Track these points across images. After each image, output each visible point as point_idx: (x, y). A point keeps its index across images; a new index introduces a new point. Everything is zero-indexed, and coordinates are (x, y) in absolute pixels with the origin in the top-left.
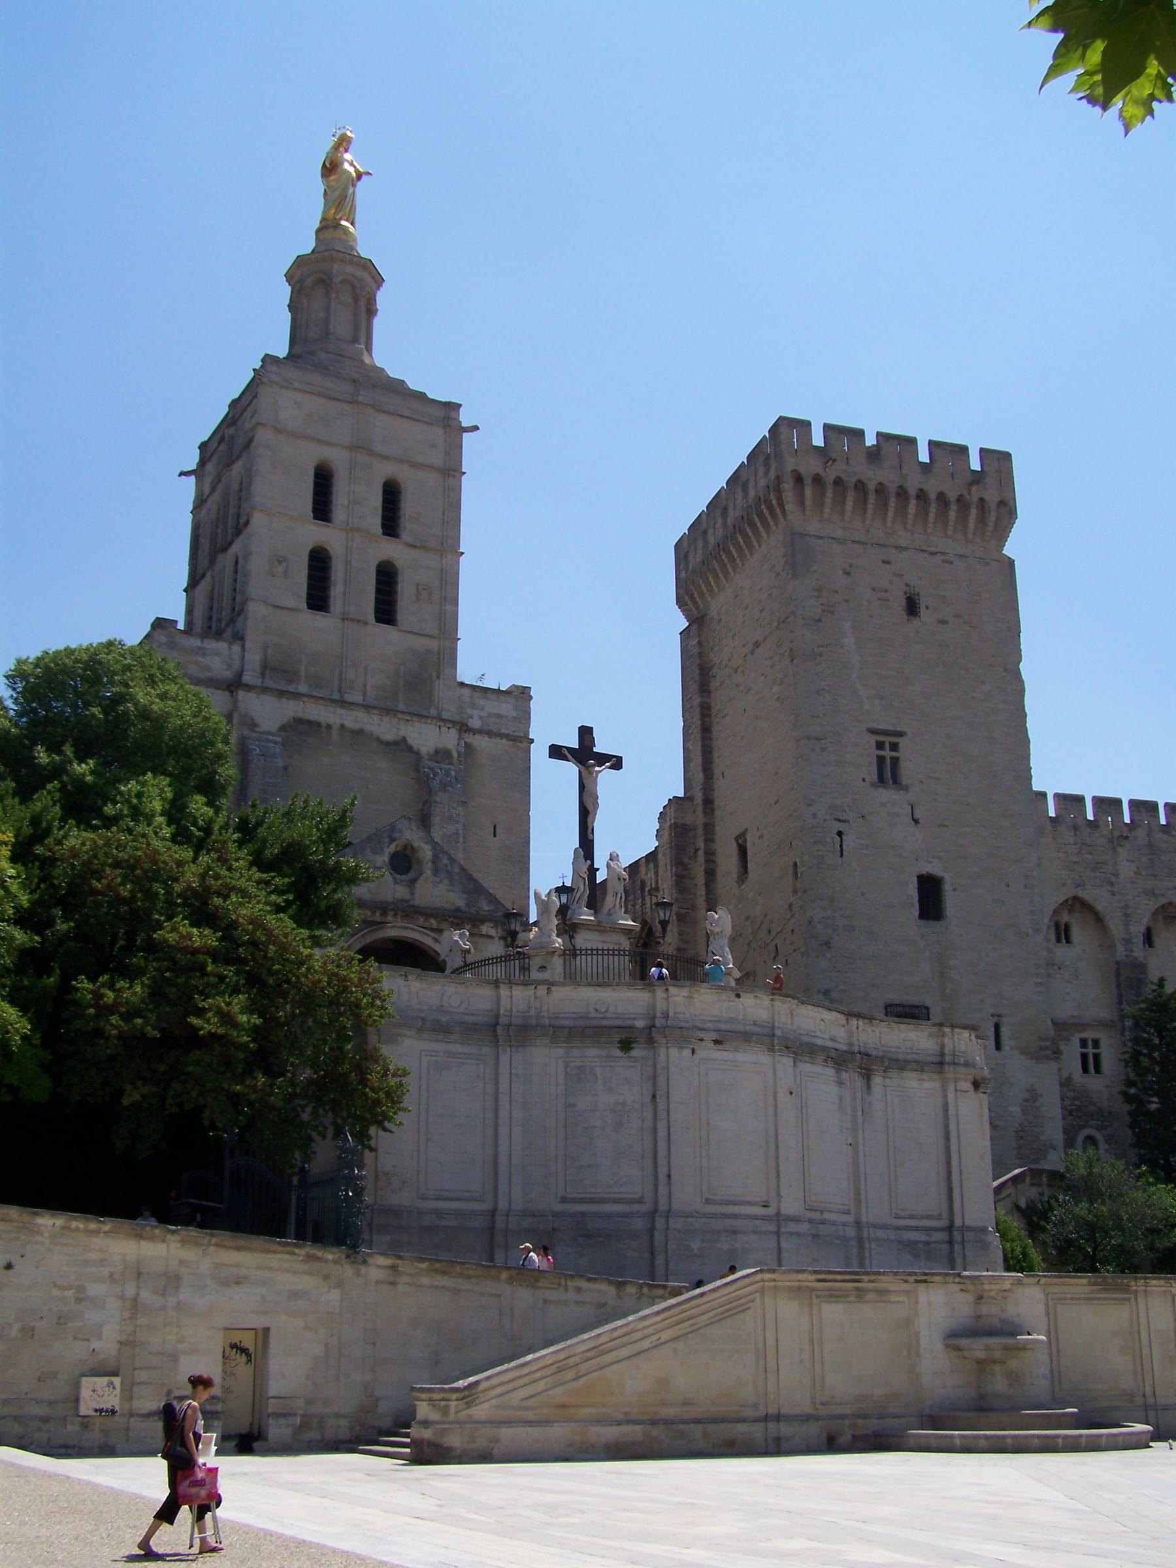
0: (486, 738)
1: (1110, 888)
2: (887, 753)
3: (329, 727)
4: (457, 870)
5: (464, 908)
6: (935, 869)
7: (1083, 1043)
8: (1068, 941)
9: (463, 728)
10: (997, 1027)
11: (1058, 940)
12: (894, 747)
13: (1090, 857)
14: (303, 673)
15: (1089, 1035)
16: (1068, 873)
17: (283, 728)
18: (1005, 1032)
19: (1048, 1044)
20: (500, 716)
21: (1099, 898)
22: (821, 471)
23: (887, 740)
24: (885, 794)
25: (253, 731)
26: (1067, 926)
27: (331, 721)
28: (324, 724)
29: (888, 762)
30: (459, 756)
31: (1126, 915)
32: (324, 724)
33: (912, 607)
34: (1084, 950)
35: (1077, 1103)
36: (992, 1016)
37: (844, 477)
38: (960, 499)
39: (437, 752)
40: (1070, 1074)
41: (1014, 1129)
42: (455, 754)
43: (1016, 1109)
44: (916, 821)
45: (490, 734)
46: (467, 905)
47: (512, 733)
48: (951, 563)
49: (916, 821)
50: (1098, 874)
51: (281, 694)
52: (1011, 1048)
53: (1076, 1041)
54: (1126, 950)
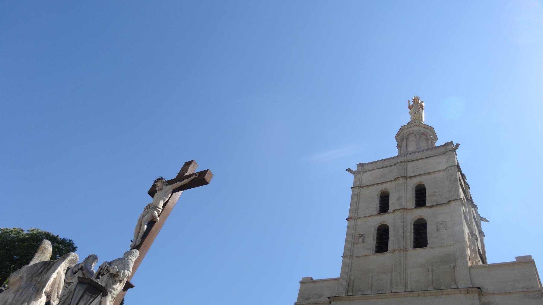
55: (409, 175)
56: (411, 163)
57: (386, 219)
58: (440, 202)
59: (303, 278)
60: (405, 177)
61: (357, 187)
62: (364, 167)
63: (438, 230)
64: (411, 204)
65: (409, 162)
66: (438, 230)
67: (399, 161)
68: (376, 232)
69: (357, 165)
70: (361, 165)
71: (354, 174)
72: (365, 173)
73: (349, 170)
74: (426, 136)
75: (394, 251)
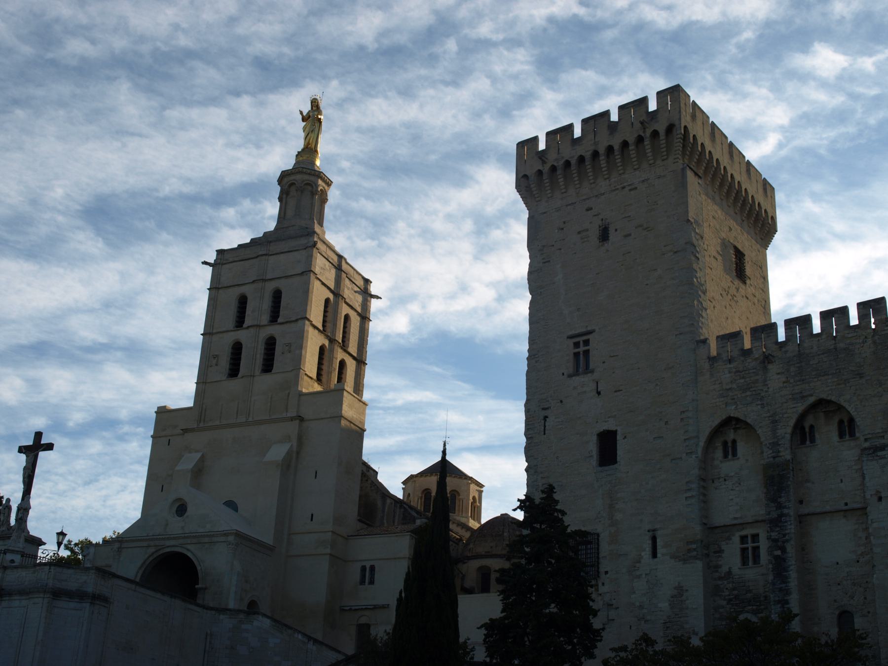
1: (759, 402)
2: (582, 349)
6: (610, 426)
7: (743, 539)
8: (735, 454)
9: (301, 419)
10: (654, 539)
11: (726, 456)
12: (587, 342)
13: (742, 381)
15: (749, 531)
16: (723, 399)
18: (659, 542)
19: (694, 546)
21: (750, 413)
22: (541, 168)
23: (581, 339)
24: (577, 379)
26: (734, 442)
29: (581, 356)
31: (774, 422)
33: (604, 235)
34: (747, 460)
35: (735, 592)
36: (649, 531)
37: (556, 164)
38: (640, 140)
40: (730, 568)
41: (662, 622)
43: (665, 605)
44: (599, 393)
48: (636, 188)
49: (599, 393)
50: (748, 393)
52: (663, 555)
53: (736, 539)
54: (773, 452)
55: (268, 277)
56: (272, 256)
57: (242, 335)
58: (290, 318)
59: (158, 408)
60: (264, 280)
61: (215, 288)
62: (224, 254)
63: (283, 353)
64: (265, 319)
65: (271, 255)
66: (283, 353)
67: (260, 253)
68: (230, 350)
69: (216, 251)
70: (220, 252)
71: (211, 266)
72: (225, 266)
73: (205, 263)
74: (312, 187)
75: (242, 377)
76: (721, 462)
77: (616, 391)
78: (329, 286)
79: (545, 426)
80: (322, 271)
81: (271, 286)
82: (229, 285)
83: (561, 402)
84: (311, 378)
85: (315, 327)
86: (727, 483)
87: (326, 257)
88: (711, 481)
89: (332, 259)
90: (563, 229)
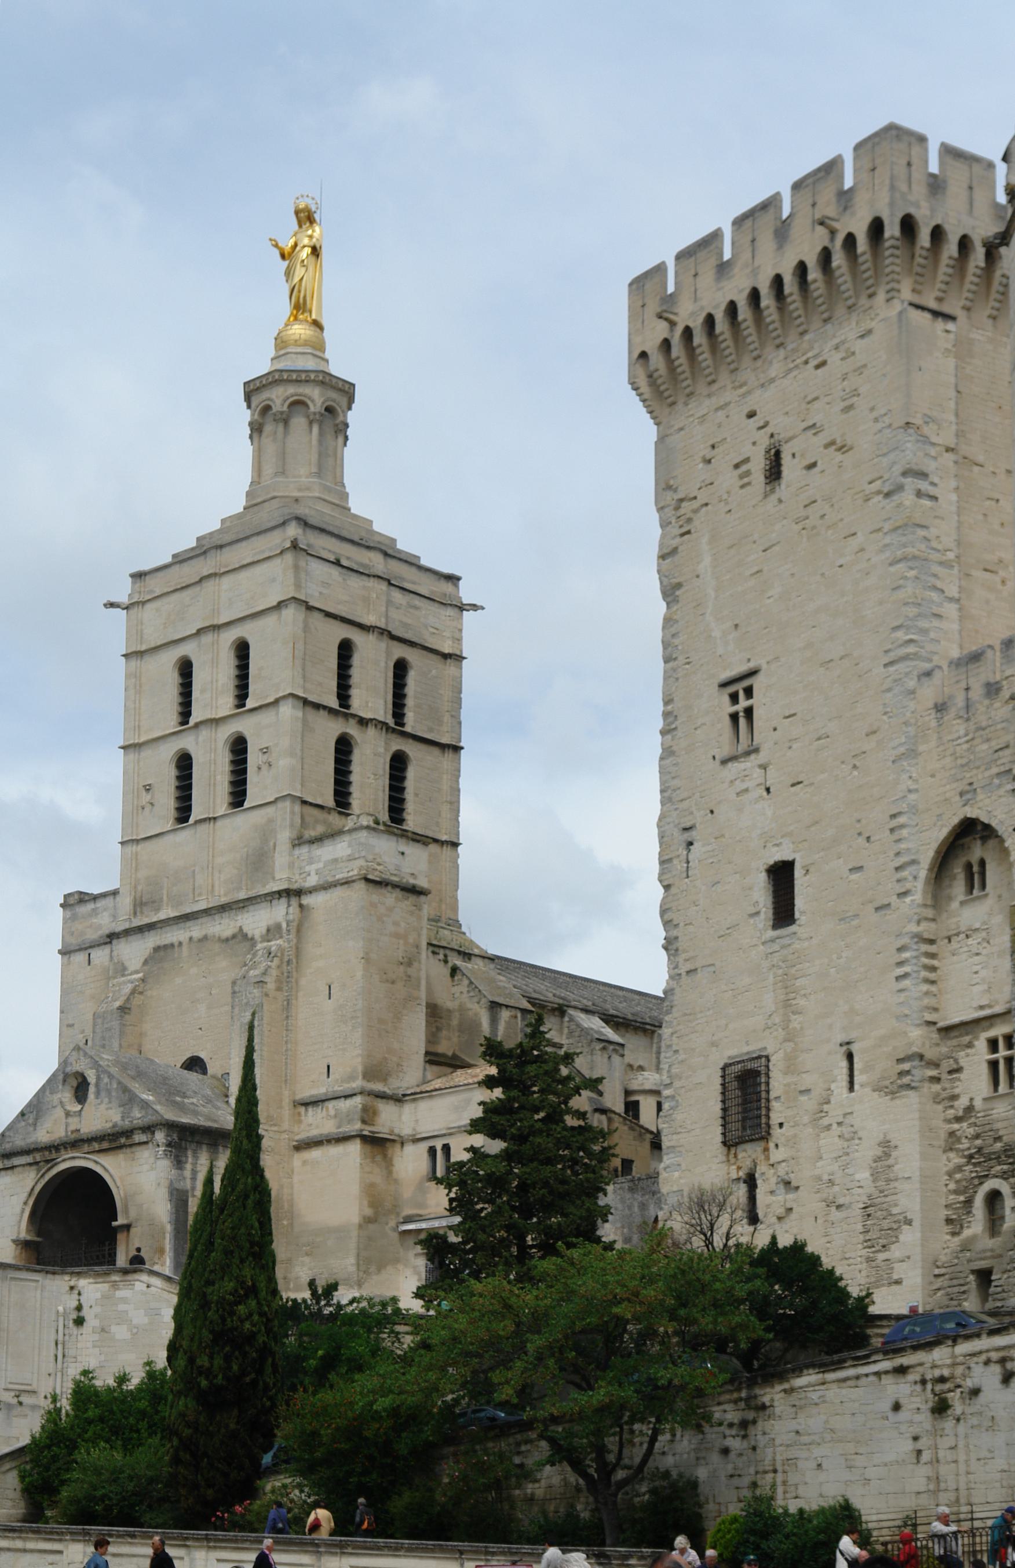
0: (323, 892)
3: (180, 944)
4: (115, 1086)
5: (120, 1123)
8: (983, 886)
12: (749, 692)
14: (165, 898)
17: (146, 962)
20: (335, 861)
23: (739, 687)
25: (123, 975)
26: (982, 863)
27: (181, 939)
28: (176, 944)
30: (288, 925)
32: (176, 944)
36: (841, 1045)
39: (268, 930)
42: (284, 925)
44: (768, 790)
45: (326, 887)
46: (123, 1119)
47: (345, 875)
49: (768, 790)
51: (141, 930)
76: (962, 903)
77: (793, 785)
78: (344, 614)
79: (688, 862)
80: (325, 591)
81: (230, 636)
82: (159, 644)
83: (712, 812)
84: (321, 807)
85: (317, 706)
86: (970, 941)
87: (332, 559)
88: (946, 941)
89: (348, 558)
90: (709, 461)
